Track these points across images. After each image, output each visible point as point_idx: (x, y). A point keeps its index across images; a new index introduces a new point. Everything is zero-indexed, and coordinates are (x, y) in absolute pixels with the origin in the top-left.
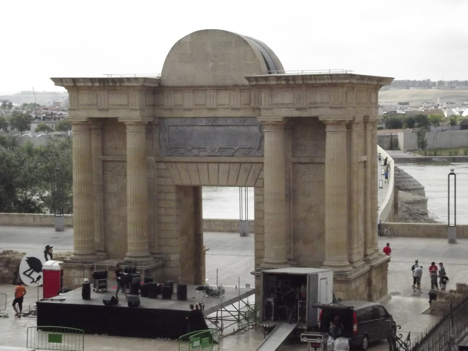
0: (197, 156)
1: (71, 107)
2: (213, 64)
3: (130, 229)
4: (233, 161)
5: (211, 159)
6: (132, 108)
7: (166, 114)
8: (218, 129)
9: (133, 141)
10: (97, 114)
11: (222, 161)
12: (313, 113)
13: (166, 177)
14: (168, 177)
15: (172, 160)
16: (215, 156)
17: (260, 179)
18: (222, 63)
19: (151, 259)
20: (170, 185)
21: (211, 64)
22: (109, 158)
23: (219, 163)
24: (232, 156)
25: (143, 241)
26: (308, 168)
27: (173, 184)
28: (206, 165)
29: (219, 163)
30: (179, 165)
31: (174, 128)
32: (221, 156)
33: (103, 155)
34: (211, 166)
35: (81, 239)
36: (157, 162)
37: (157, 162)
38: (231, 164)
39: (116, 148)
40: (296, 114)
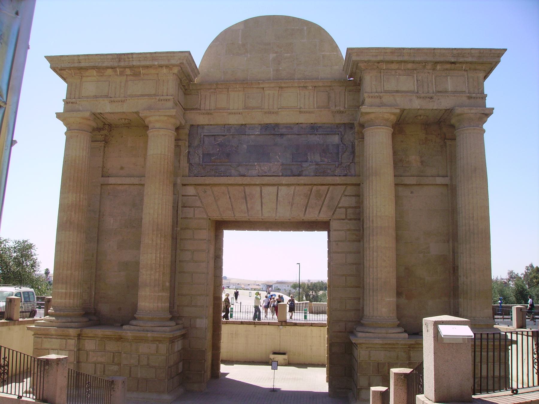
0: (244, 176)
1: (70, 100)
2: (275, 55)
3: (146, 275)
4: (302, 182)
5: (266, 180)
6: (162, 98)
7: (201, 120)
8: (278, 139)
9: (160, 145)
10: (106, 107)
11: (284, 183)
12: (445, 103)
13: (196, 207)
14: (198, 207)
15: (207, 182)
16: (273, 176)
17: (340, 208)
18: (289, 55)
19: (173, 323)
20: (199, 219)
21: (272, 56)
22: (112, 180)
23: (278, 185)
24: (299, 175)
25: (164, 294)
26: (412, 193)
27: (205, 217)
28: (258, 188)
29: (278, 185)
30: (216, 189)
31: (212, 138)
32: (282, 176)
33: (102, 177)
34: (266, 190)
35: (64, 291)
36: (184, 185)
37: (184, 185)
38: (298, 188)
39: (122, 168)
40: (416, 104)
